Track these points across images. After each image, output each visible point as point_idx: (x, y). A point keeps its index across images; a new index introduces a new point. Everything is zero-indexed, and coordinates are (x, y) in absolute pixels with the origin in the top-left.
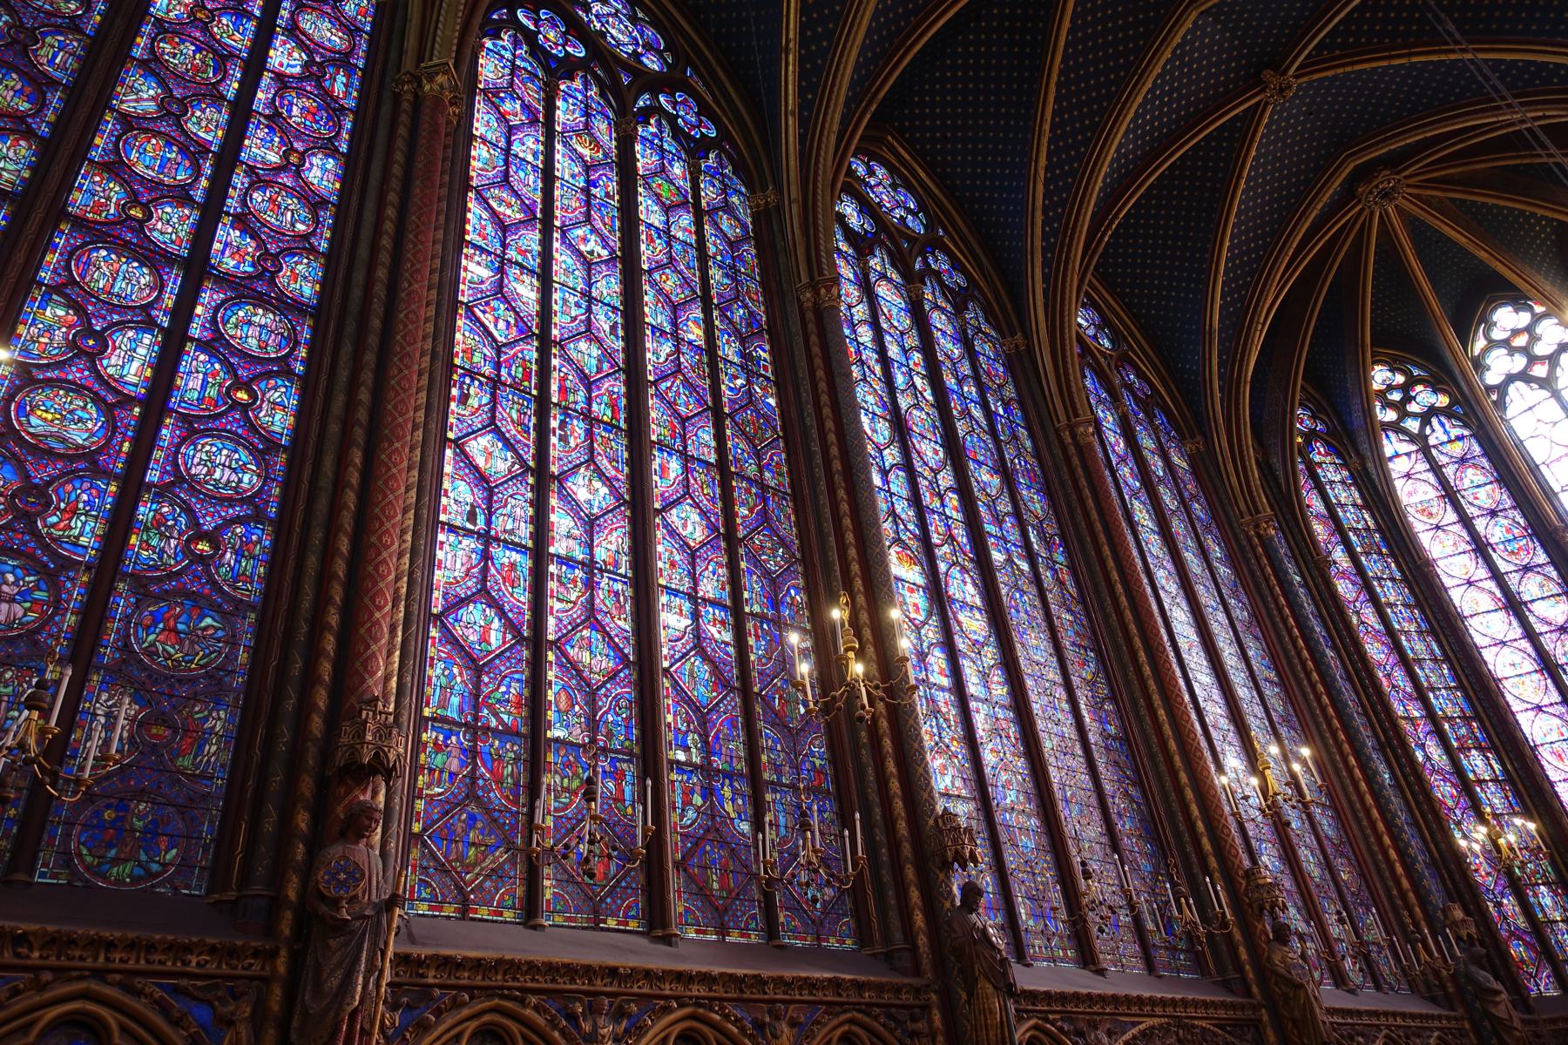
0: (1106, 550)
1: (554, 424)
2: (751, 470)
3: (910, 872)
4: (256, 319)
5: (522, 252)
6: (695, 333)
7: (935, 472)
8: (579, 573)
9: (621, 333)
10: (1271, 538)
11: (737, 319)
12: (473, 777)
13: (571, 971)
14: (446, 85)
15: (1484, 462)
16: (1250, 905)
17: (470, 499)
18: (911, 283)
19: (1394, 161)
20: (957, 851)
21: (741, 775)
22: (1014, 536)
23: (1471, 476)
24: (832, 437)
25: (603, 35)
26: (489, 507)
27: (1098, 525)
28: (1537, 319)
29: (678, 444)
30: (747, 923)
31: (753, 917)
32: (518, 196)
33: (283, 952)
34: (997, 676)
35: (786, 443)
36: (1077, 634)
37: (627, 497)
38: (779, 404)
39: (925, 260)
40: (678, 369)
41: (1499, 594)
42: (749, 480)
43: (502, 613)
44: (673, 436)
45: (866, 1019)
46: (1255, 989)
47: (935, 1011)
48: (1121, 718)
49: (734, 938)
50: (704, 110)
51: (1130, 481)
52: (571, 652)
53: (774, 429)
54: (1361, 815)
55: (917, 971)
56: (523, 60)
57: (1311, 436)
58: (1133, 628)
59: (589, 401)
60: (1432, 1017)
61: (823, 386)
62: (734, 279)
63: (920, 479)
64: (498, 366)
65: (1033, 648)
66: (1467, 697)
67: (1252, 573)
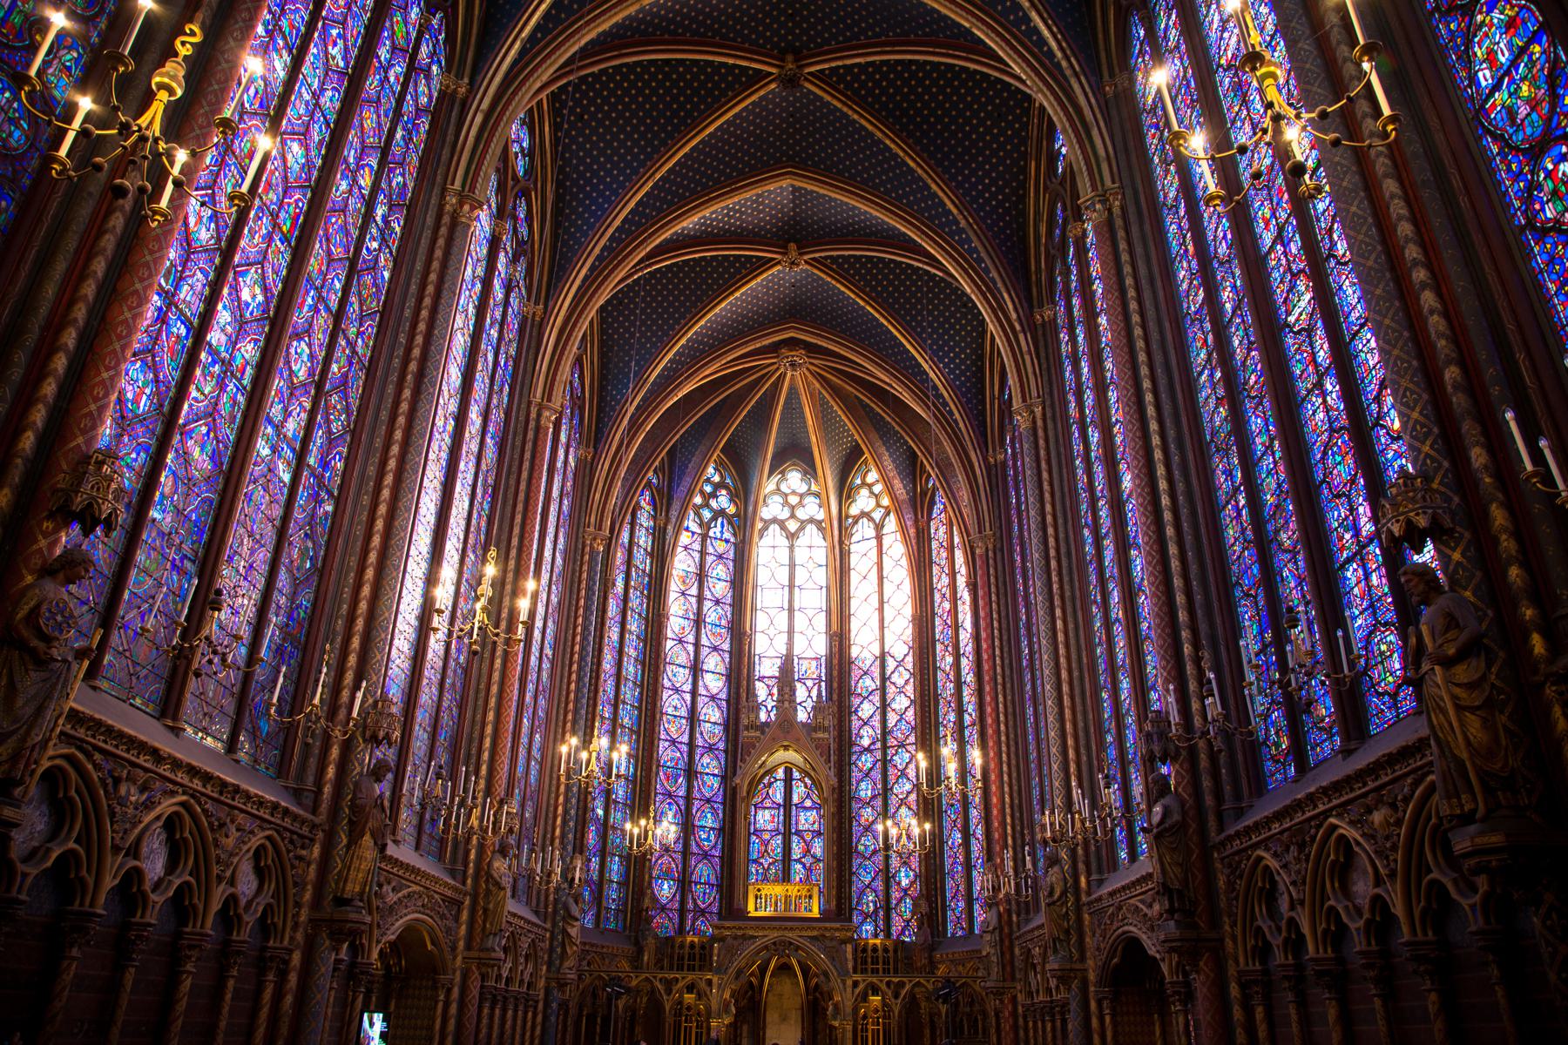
2: (352, 331)
6: (366, 181)
18: (500, 214)
19: (812, 349)
22: (470, 477)
24: (419, 339)
28: (809, 493)
38: (391, 279)
40: (344, 210)
46: (469, 881)
52: (190, 443)
55: (314, 812)
57: (649, 483)
61: (430, 289)
66: (639, 717)
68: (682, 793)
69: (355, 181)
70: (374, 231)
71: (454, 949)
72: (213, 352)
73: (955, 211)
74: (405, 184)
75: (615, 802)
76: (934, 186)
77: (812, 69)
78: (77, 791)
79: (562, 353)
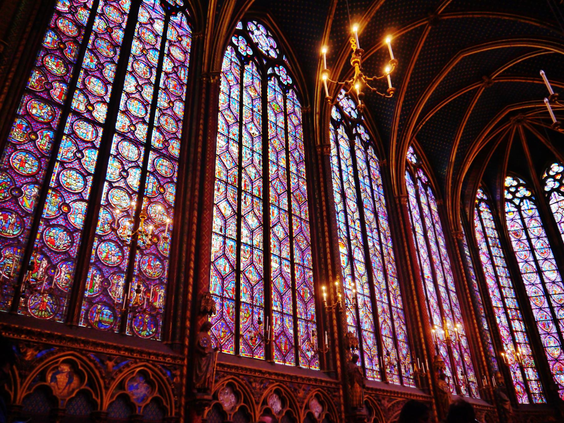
1: (243, 197)
4: (164, 164)
5: (234, 135)
6: (283, 163)
8: (249, 249)
9: (261, 164)
11: (296, 157)
12: (222, 311)
13: (251, 370)
15: (539, 219)
18: (352, 138)
21: (291, 315)
22: (376, 236)
23: (533, 223)
26: (225, 227)
29: (277, 204)
31: (292, 358)
33: (186, 359)
34: (366, 286)
36: (392, 272)
38: (307, 188)
41: (535, 267)
42: (297, 216)
43: (229, 262)
44: (276, 201)
45: (322, 391)
46: (432, 393)
50: (289, 73)
52: (247, 275)
54: (475, 340)
55: (337, 378)
57: (481, 200)
60: (485, 406)
62: (296, 141)
63: (348, 216)
64: (227, 177)
65: (379, 276)
66: (518, 302)
68: (554, 330)
69: (278, 165)
72: (246, 244)
73: (538, 25)
74: (300, 154)
75: (519, 343)
76: (522, 21)
77: (440, 12)
78: (239, 387)
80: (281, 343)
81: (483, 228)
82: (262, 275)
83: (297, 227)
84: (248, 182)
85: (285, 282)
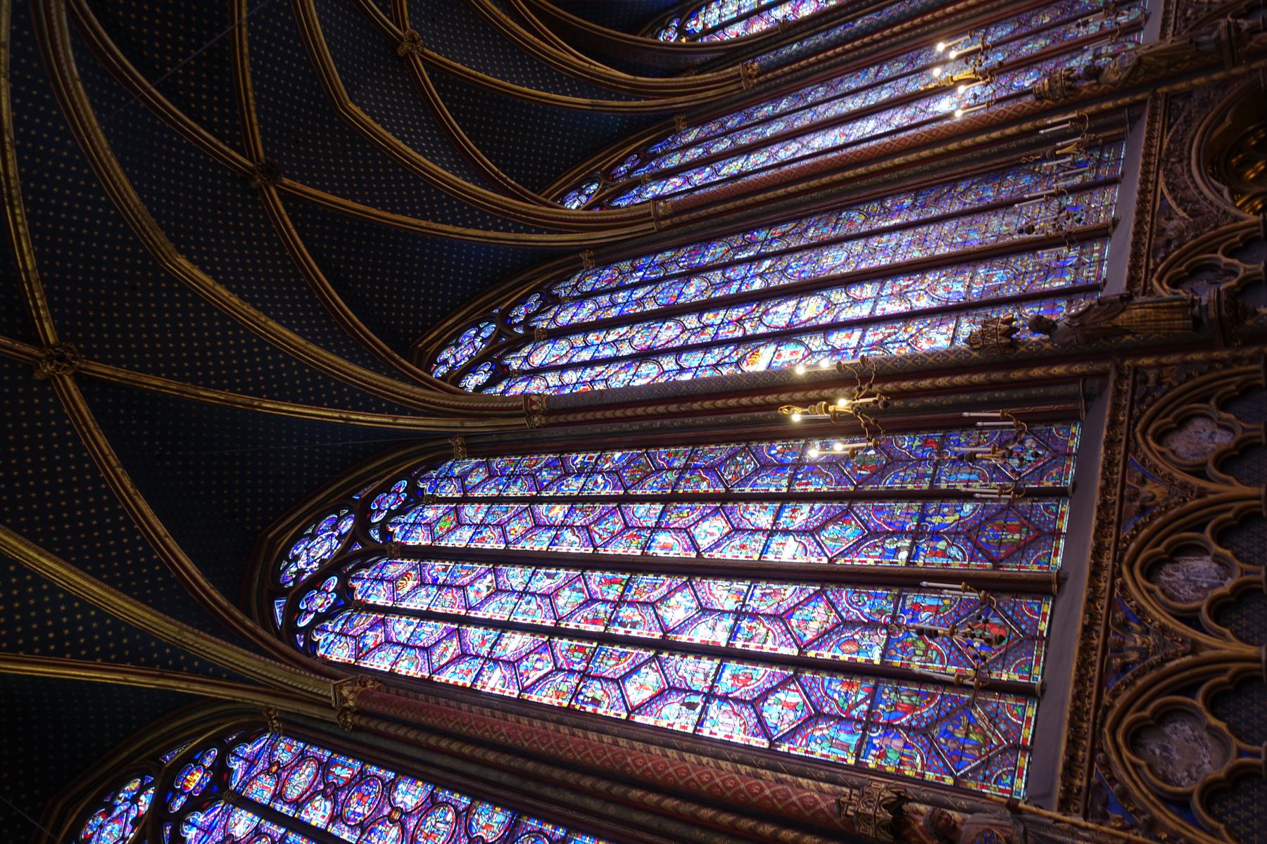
0: (760, 197)
1: (621, 631)
2: (671, 477)
3: (1017, 375)
5: (484, 642)
6: (558, 512)
7: (684, 329)
9: (553, 571)
10: (760, 66)
11: (550, 477)
12: (909, 729)
13: (1084, 664)
14: (350, 688)
16: (1066, 97)
17: (677, 706)
18: (533, 337)
20: (1002, 335)
22: (741, 270)
24: (650, 410)
25: (322, 561)
26: (685, 691)
27: (739, 203)
29: (647, 534)
30: (1052, 513)
31: (1046, 507)
32: (440, 641)
34: (856, 291)
35: (651, 447)
36: (826, 225)
37: (685, 579)
38: (620, 449)
39: (517, 325)
40: (586, 528)
42: (679, 479)
43: (773, 690)
44: (639, 537)
45: (1143, 420)
46: (1139, 97)
47: (1140, 362)
48: (899, 194)
49: (1064, 525)
50: (386, 488)
51: (705, 175)
52: (809, 637)
53: (639, 455)
55: (1104, 375)
56: (336, 625)
57: (681, 31)
58: (825, 180)
59: (605, 601)
61: (609, 414)
62: (518, 477)
64: (572, 672)
65: (834, 261)
67: (788, 82)
70: (590, 485)
71: (1224, 84)
72: (734, 632)
79: (607, 221)
80: (1000, 544)
81: (739, 19)
82: (811, 589)
83: (704, 480)
84: (587, 613)
85: (833, 520)
